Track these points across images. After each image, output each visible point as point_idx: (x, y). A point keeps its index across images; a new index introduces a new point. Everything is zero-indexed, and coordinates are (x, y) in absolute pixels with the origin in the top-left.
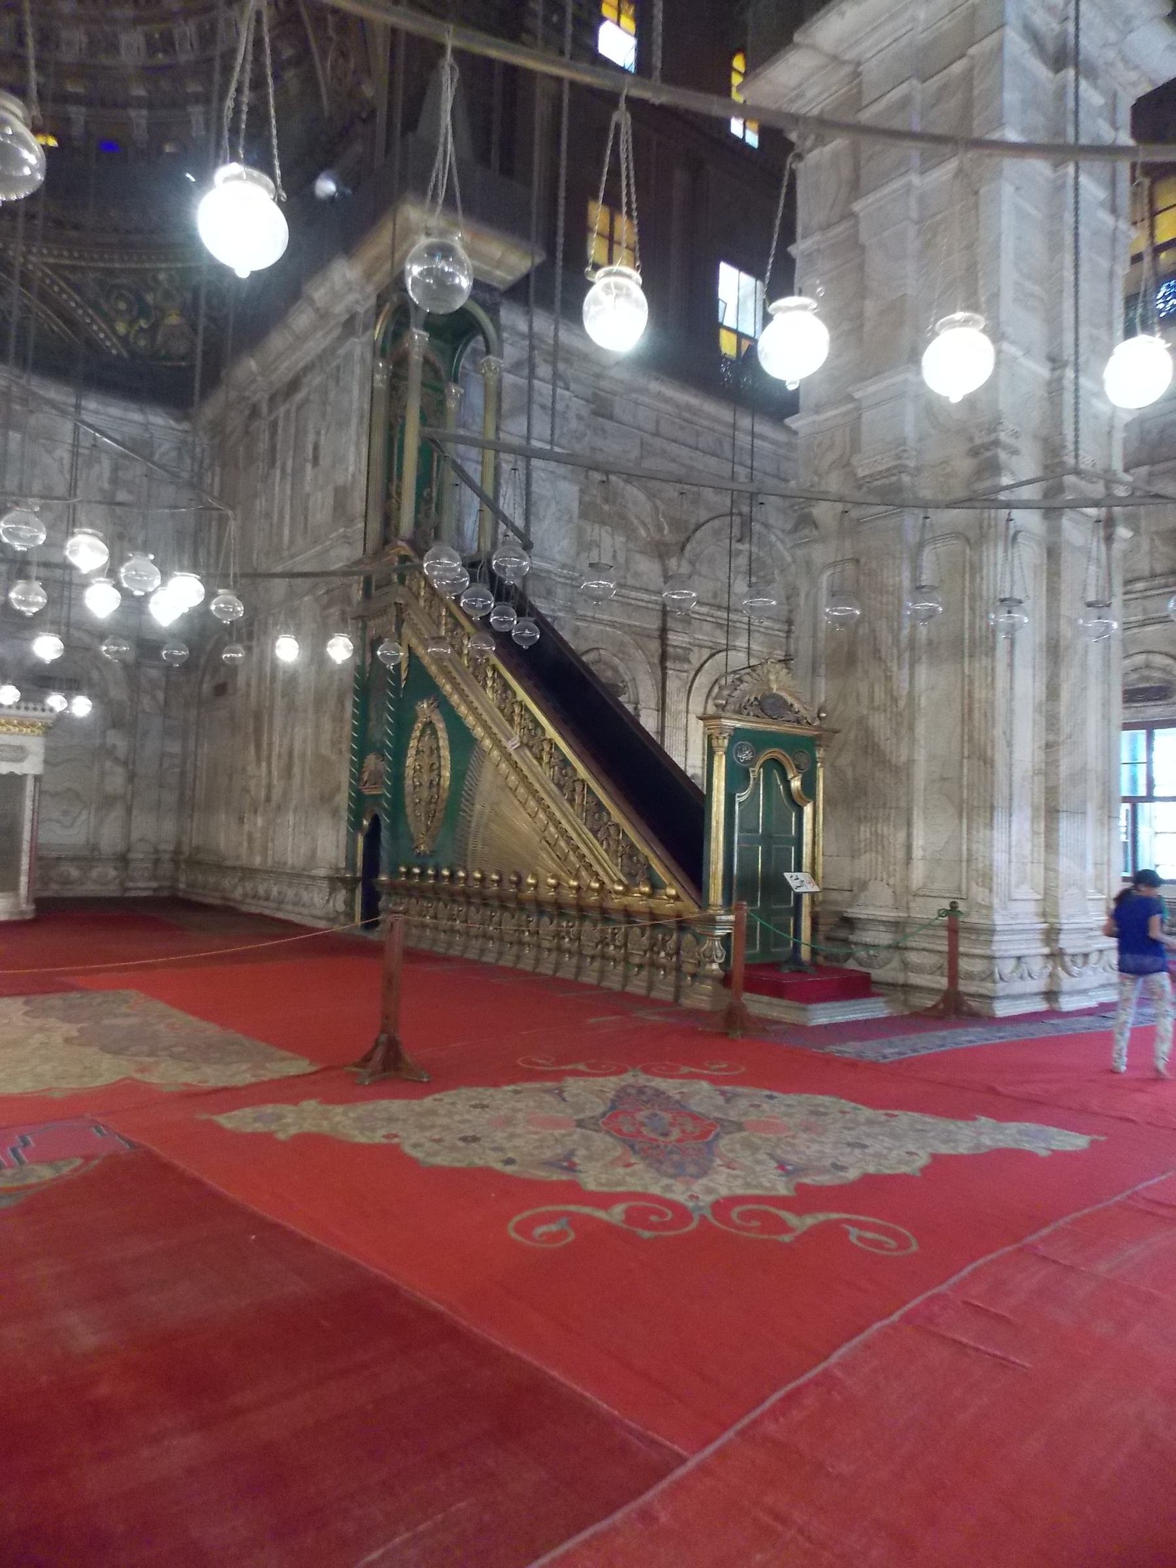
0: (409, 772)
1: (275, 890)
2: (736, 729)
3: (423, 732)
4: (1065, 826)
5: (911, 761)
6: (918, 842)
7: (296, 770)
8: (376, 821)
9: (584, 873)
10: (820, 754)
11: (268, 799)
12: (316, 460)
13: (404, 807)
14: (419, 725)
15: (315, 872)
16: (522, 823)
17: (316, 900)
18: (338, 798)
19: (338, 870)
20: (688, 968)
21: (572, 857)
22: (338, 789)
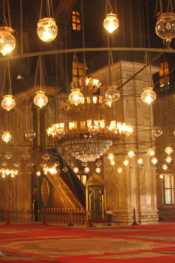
0: (42, 191)
1: (15, 215)
2: (89, 185)
3: (44, 184)
4: (142, 197)
5: (118, 187)
6: (120, 200)
7: (19, 191)
8: (36, 201)
9: (71, 207)
10: (105, 187)
11: (13, 197)
12: (19, 127)
13: (41, 198)
14: (43, 183)
15: (25, 211)
16: (63, 200)
17: (25, 216)
18: (28, 196)
19: (29, 210)
20: (84, 220)
21: (69, 205)
22: (28, 194)
